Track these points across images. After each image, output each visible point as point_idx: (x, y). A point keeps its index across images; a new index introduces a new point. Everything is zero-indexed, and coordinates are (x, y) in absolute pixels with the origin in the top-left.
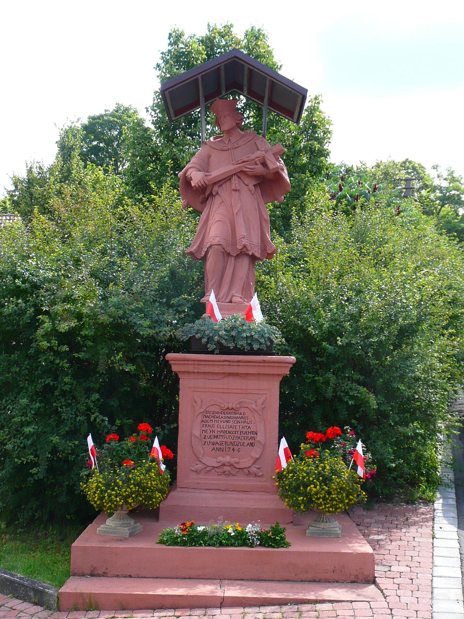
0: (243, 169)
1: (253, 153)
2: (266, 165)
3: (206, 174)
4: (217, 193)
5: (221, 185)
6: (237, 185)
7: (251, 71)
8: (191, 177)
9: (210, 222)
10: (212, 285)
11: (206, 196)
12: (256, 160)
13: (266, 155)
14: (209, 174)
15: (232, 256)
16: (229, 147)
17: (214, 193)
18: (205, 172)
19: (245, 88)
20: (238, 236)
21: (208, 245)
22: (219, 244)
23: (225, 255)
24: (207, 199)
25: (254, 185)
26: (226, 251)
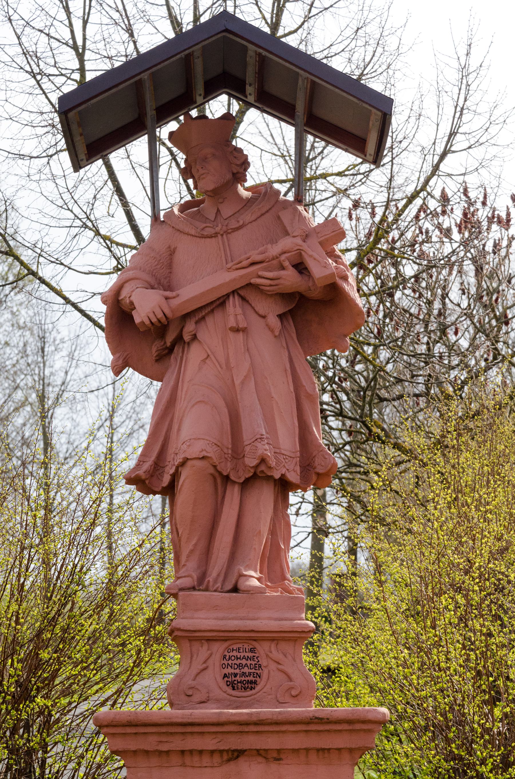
0: (253, 281)
1: (274, 241)
2: (306, 268)
3: (168, 294)
4: (195, 337)
5: (203, 318)
6: (240, 318)
7: (262, 61)
8: (132, 303)
9: (181, 405)
10: (192, 551)
11: (168, 344)
12: (283, 257)
13: (305, 246)
14: (174, 294)
15: (234, 482)
16: (218, 229)
17: (187, 337)
18: (165, 290)
19: (249, 89)
20: (247, 436)
21: (179, 460)
22: (203, 458)
23: (219, 480)
24: (171, 350)
25: (281, 317)
26: (220, 473)
